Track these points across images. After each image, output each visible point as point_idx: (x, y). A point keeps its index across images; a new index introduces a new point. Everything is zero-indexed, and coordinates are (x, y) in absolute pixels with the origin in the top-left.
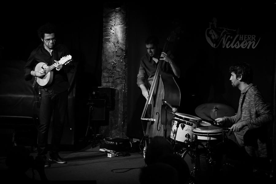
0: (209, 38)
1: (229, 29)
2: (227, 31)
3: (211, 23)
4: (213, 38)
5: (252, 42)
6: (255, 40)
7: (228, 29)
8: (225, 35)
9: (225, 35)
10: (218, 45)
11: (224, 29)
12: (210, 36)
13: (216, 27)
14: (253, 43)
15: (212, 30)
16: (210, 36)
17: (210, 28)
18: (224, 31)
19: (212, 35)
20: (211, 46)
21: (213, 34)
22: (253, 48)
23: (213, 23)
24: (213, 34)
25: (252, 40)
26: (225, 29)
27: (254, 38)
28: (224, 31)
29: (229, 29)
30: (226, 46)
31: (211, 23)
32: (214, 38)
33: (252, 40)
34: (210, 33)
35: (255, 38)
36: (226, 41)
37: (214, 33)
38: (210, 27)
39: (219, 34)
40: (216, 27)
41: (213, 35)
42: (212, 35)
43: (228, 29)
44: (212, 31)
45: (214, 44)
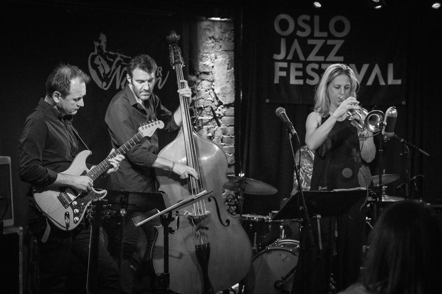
0: (94, 71)
1: (125, 57)
2: (122, 60)
3: (97, 44)
4: (102, 72)
5: (158, 78)
6: (161, 75)
7: (123, 56)
8: (120, 67)
9: (120, 67)
10: (110, 84)
11: (117, 56)
12: (95, 67)
13: (105, 51)
14: (159, 80)
15: (99, 56)
16: (95, 67)
17: (96, 53)
18: (118, 59)
19: (99, 66)
20: (97, 85)
21: (102, 64)
22: (160, 88)
23: (101, 45)
24: (102, 64)
25: (158, 75)
26: (119, 55)
27: (160, 72)
28: (118, 59)
29: (125, 57)
30: (120, 86)
31: (97, 44)
32: (103, 71)
33: (158, 75)
34: (97, 62)
35: (162, 72)
36: (121, 79)
37: (103, 62)
38: (96, 50)
39: (110, 64)
40: (105, 51)
41: (100, 65)
42: (99, 66)
43: (123, 56)
44: (100, 61)
45: (102, 80)
